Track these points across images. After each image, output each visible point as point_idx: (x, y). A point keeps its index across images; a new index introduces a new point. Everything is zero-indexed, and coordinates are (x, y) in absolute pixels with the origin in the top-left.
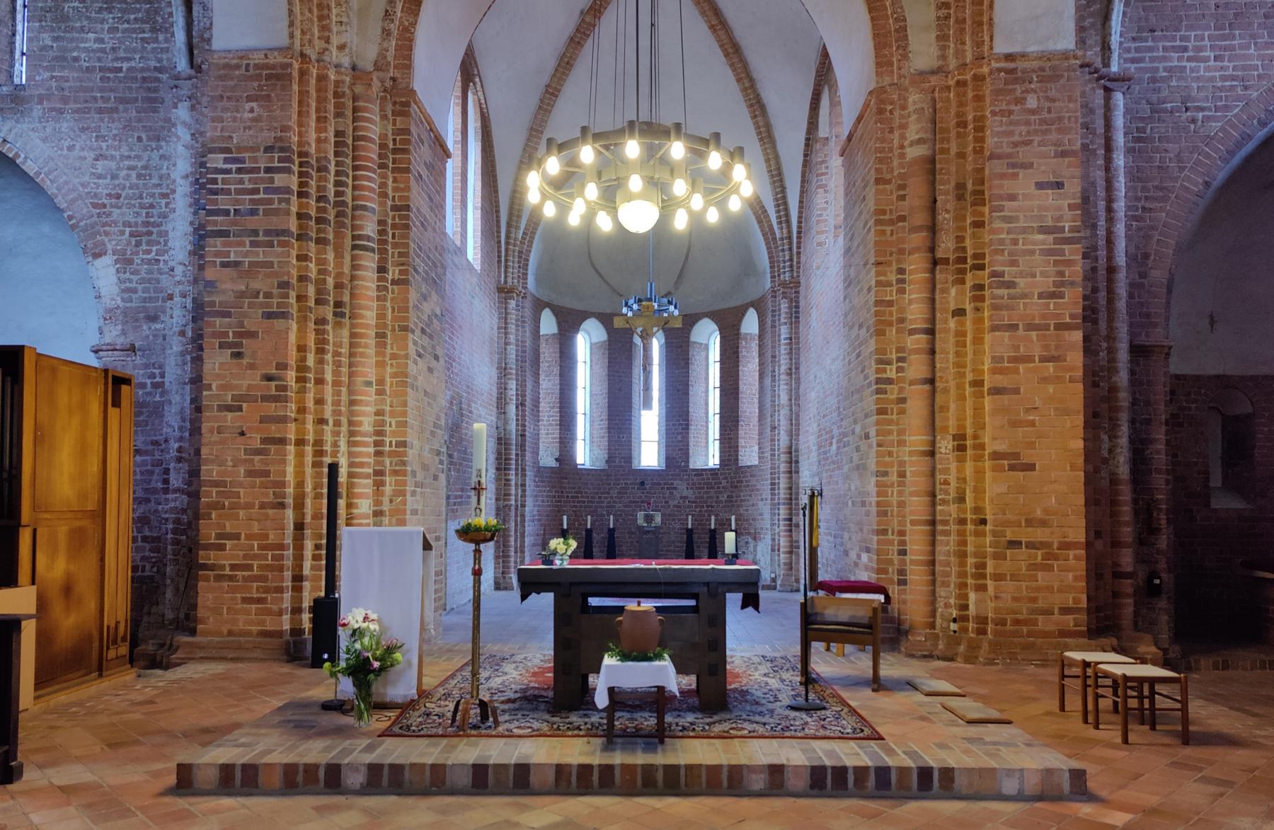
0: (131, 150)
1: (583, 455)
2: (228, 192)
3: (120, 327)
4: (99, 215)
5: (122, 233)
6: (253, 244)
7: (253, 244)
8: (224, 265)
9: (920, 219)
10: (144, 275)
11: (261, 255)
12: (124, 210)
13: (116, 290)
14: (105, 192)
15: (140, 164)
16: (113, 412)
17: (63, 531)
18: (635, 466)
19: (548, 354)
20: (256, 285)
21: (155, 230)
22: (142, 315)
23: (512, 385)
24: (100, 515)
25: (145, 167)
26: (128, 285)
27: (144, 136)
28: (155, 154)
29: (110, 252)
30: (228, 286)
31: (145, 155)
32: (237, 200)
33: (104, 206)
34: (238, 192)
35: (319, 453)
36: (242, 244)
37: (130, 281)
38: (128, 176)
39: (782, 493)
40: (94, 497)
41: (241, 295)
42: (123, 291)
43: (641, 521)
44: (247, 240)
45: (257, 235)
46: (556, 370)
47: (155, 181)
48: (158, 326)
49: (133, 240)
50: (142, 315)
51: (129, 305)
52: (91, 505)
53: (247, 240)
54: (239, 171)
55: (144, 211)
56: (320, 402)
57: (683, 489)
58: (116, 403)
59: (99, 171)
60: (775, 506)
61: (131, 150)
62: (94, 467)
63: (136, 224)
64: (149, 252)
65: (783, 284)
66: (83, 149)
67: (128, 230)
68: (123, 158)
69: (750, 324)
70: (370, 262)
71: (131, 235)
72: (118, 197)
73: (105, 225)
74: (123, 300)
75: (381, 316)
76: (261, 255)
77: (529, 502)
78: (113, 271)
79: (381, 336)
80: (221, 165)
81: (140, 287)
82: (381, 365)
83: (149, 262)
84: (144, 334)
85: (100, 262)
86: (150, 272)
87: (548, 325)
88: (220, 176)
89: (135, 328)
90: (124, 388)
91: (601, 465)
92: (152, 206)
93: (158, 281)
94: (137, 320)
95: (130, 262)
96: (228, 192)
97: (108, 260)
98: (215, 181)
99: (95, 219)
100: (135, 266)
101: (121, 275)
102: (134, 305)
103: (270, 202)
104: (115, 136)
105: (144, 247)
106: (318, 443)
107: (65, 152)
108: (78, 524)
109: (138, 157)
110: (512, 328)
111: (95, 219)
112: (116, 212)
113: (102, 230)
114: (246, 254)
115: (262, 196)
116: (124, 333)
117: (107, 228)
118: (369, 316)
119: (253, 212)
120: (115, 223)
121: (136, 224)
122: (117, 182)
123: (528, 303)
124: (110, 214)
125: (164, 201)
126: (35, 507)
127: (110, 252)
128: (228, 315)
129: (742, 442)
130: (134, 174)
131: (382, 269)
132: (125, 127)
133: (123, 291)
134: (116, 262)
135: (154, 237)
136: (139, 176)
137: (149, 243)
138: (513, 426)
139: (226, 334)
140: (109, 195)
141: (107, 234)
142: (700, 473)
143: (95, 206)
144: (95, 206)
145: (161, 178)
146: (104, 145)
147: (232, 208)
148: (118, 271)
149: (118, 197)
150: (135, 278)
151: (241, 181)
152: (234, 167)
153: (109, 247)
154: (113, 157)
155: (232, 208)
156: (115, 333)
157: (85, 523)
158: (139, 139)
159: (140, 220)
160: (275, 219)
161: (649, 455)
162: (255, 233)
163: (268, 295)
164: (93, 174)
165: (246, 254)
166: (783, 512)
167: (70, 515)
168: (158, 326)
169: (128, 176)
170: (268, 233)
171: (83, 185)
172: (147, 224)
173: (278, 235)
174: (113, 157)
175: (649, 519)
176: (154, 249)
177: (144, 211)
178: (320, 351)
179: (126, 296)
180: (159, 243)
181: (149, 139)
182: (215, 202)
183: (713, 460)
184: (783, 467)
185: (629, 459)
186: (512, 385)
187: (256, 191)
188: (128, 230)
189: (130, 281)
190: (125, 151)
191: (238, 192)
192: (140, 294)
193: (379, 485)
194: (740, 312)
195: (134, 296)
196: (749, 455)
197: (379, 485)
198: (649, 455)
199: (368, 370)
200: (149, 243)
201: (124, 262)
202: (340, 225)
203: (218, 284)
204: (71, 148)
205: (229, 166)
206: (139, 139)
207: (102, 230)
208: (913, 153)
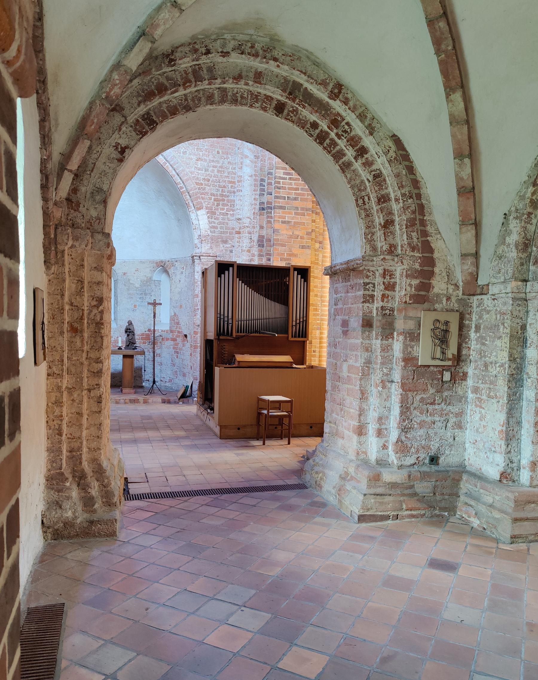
0: (214, 157)
2: (284, 188)
3: (209, 245)
4: (199, 189)
5: (211, 199)
6: (296, 214)
7: (296, 214)
8: (283, 222)
11: (299, 219)
14: (202, 177)
15: (218, 165)
20: (297, 233)
21: (226, 199)
22: (220, 240)
25: (221, 167)
27: (220, 152)
28: (226, 161)
29: (204, 207)
30: (285, 232)
31: (221, 161)
32: (289, 193)
33: (202, 184)
34: (290, 189)
36: (290, 213)
37: (214, 223)
38: (213, 170)
41: (290, 237)
42: (211, 227)
44: (293, 212)
45: (298, 209)
47: (226, 174)
48: (227, 246)
49: (216, 203)
50: (220, 240)
51: (213, 234)
53: (293, 212)
54: (290, 179)
55: (221, 189)
59: (199, 166)
61: (214, 157)
64: (223, 209)
66: (190, 154)
68: (210, 161)
71: (215, 200)
73: (202, 194)
74: (211, 232)
76: (299, 219)
80: (282, 175)
81: (219, 226)
83: (223, 214)
84: (221, 249)
85: (199, 212)
86: (223, 219)
88: (281, 181)
89: (217, 246)
92: (224, 187)
93: (227, 224)
94: (218, 242)
95: (214, 213)
96: (284, 188)
98: (279, 183)
99: (197, 190)
100: (216, 216)
101: (210, 220)
102: (216, 235)
103: (303, 195)
104: (206, 149)
105: (221, 206)
107: (182, 154)
109: (218, 162)
111: (197, 190)
112: (207, 188)
113: (201, 196)
114: (293, 218)
115: (300, 192)
116: (211, 248)
119: (295, 199)
120: (207, 193)
121: (217, 194)
122: (208, 173)
124: (204, 189)
125: (230, 185)
127: (204, 207)
128: (284, 245)
130: (216, 170)
132: (211, 145)
133: (211, 227)
134: (208, 213)
135: (225, 202)
136: (218, 171)
139: (283, 254)
140: (204, 179)
141: (203, 198)
145: (229, 173)
146: (201, 153)
147: (286, 196)
148: (208, 217)
150: (216, 221)
151: (291, 184)
152: (288, 177)
154: (205, 160)
155: (286, 196)
156: (207, 248)
158: (218, 152)
159: (219, 193)
160: (305, 203)
162: (297, 208)
163: (302, 238)
164: (196, 167)
165: (293, 218)
168: (227, 246)
169: (213, 171)
170: (302, 209)
171: (191, 173)
172: (222, 195)
173: (307, 210)
174: (205, 160)
176: (225, 208)
179: (212, 230)
180: (228, 205)
181: (223, 153)
182: (279, 193)
187: (297, 189)
188: (213, 197)
189: (214, 223)
190: (211, 157)
191: (290, 189)
192: (219, 229)
200: (223, 205)
201: (211, 213)
203: (280, 231)
204: (185, 153)
205: (285, 176)
206: (218, 152)
207: (201, 196)
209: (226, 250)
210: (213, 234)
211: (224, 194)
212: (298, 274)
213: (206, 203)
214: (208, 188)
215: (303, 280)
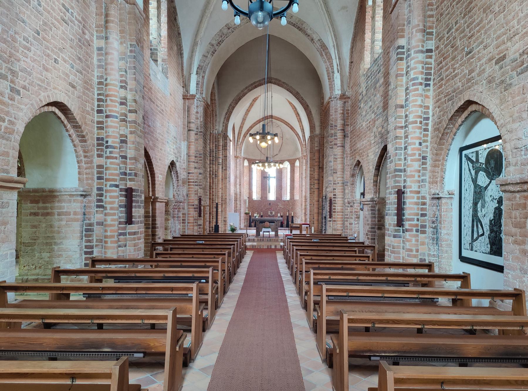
1: (256, 196)
9: (317, 160)
18: (268, 199)
19: (246, 171)
23: (238, 180)
35: (213, 201)
39: (303, 207)
43: (269, 214)
46: (248, 175)
56: (213, 192)
57: (280, 206)
60: (302, 210)
65: (304, 156)
69: (297, 164)
70: (220, 167)
75: (222, 176)
77: (242, 209)
79: (222, 180)
82: (222, 185)
87: (246, 163)
91: (259, 199)
106: (213, 199)
110: (238, 166)
118: (220, 177)
123: (242, 160)
129: (295, 194)
131: (222, 168)
138: (238, 190)
142: (284, 201)
161: (272, 196)
166: (303, 211)
175: (271, 213)
178: (213, 183)
183: (288, 198)
184: (304, 200)
185: (266, 198)
186: (238, 180)
193: (222, 206)
194: (295, 160)
196: (297, 197)
197: (222, 206)
198: (272, 196)
199: (220, 186)
202: (216, 161)
208: (316, 148)
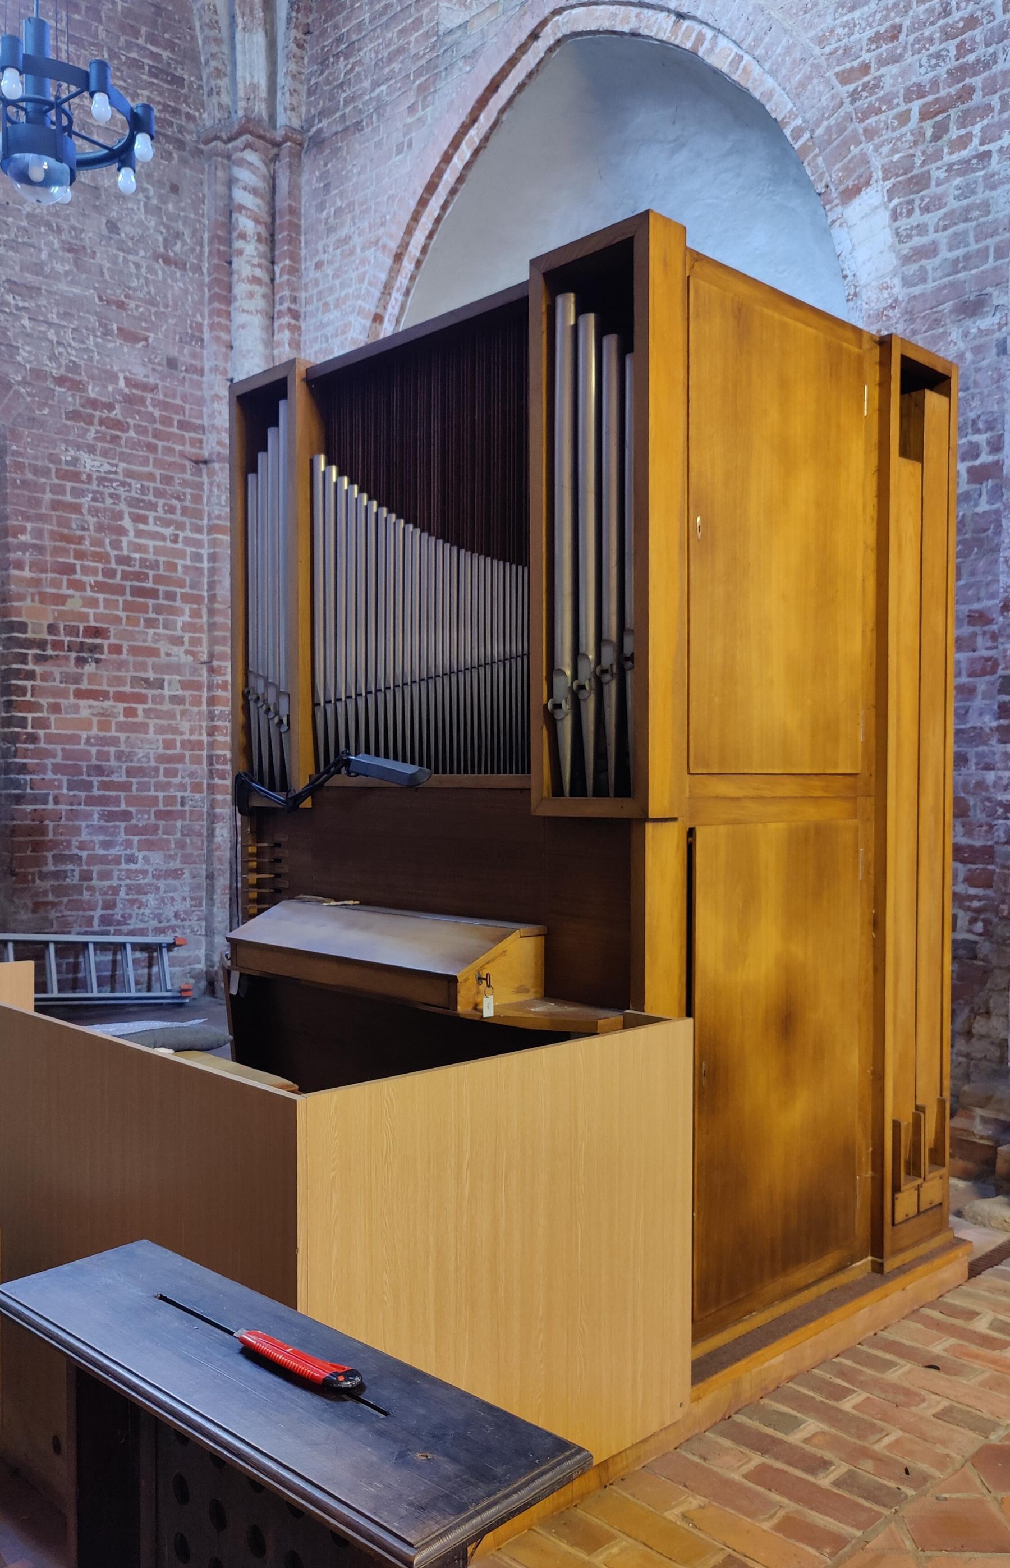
4: (854, 96)
10: (952, 204)
12: (909, 59)
13: (891, 260)
16: (900, 468)
17: (771, 836)
22: (947, 306)
24: (871, 785)
26: (917, 241)
40: (856, 733)
42: (906, 260)
50: (947, 306)
52: (848, 758)
58: (913, 448)
62: (854, 643)
63: (935, 83)
64: (963, 142)
67: (916, 106)
71: (924, 116)
72: (895, 33)
78: (885, 216)
83: (966, 167)
90: (932, 400)
94: (937, 322)
97: (873, 196)
99: (848, 108)
100: (933, 190)
105: (954, 133)
108: (811, 814)
111: (848, 108)
117: (872, 121)
120: (888, 100)
126: (691, 764)
127: (878, 174)
134: (891, 193)
135: (977, 98)
137: (964, 121)
140: (876, 39)
141: (870, 134)
143: (844, 78)
144: (844, 78)
148: (895, 216)
149: (895, 33)
150: (931, 219)
153: (877, 163)
157: (833, 812)
159: (942, 71)
167: (789, 788)
172: (958, 74)
176: (977, 129)
177: (952, 45)
179: (913, 268)
188: (916, 106)
192: (945, 254)
195: (929, 264)
201: (909, 184)
209: (978, 350)
210: (917, 290)
211: (971, 58)
212: (580, 311)
213: (885, 150)
214: (894, 69)
215: (611, 342)
